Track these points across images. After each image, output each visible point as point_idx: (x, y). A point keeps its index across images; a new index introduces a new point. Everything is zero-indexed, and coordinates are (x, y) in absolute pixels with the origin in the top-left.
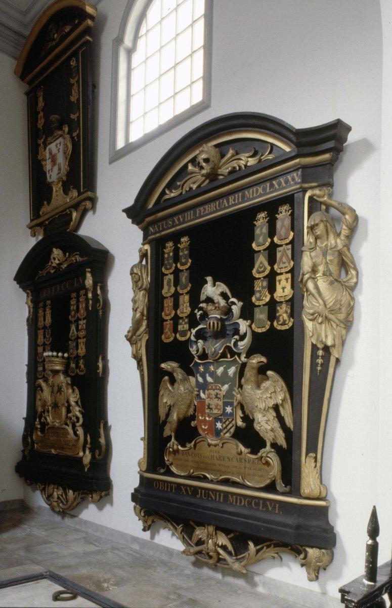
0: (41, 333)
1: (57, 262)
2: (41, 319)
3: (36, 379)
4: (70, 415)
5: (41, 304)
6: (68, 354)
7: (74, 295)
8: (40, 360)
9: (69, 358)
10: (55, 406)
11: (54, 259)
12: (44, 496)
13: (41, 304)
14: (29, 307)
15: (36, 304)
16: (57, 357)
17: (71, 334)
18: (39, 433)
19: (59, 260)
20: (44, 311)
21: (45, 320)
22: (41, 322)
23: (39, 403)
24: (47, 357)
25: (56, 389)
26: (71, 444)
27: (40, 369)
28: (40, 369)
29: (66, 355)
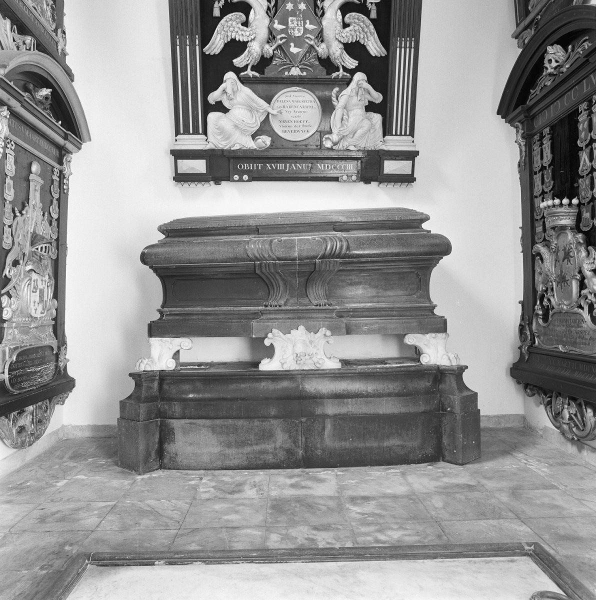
0: (537, 178)
1: (554, 64)
2: (537, 158)
3: (534, 243)
4: (584, 292)
5: (537, 137)
6: (579, 199)
7: (584, 106)
8: (539, 217)
9: (579, 205)
10: (563, 280)
11: (550, 61)
12: (550, 414)
13: (537, 137)
14: (520, 145)
15: (529, 139)
16: (561, 205)
17: (580, 168)
18: (541, 321)
19: (557, 61)
20: (542, 144)
21: (542, 158)
22: (537, 162)
23: (539, 279)
24: (545, 208)
25: (561, 254)
26: (588, 337)
27: (539, 229)
28: (539, 229)
29: (575, 201)
